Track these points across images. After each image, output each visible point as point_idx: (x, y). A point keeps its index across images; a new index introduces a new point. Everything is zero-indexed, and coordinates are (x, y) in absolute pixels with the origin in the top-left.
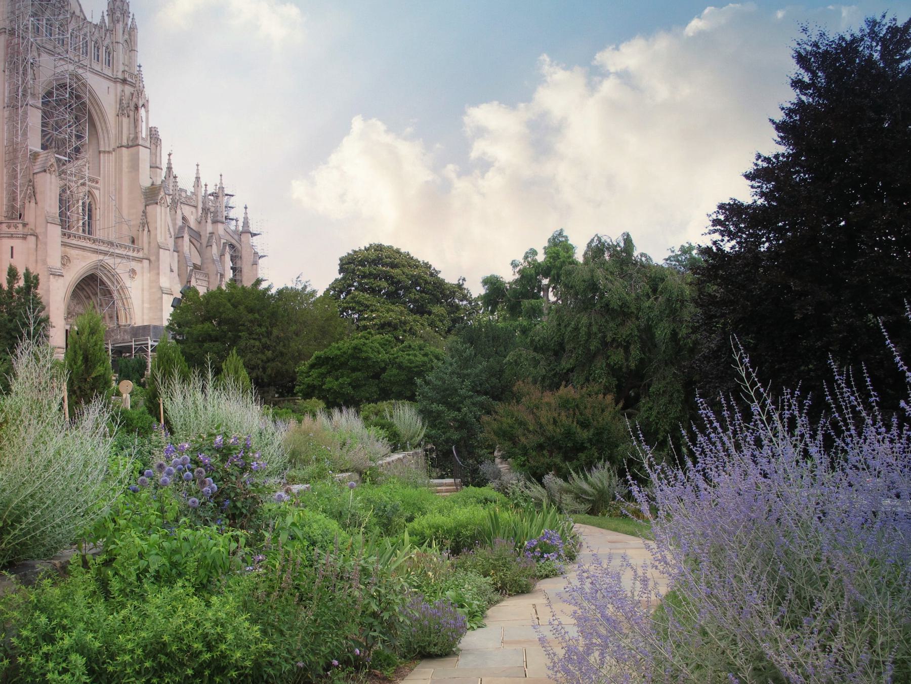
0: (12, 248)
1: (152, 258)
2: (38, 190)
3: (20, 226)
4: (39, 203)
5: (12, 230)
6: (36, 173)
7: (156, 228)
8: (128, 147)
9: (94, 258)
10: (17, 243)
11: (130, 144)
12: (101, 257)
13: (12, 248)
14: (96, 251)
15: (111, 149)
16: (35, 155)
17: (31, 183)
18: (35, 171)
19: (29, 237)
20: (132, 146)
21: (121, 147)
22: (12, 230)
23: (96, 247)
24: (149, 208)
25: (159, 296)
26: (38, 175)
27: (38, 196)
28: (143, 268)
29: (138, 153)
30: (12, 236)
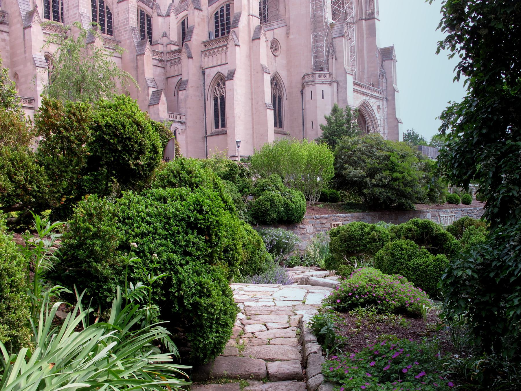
0: (323, 91)
1: (390, 98)
2: (337, 50)
3: (328, 75)
4: (339, 60)
5: (322, 79)
6: (335, 38)
7: (392, 77)
8: (366, 20)
9: (363, 98)
10: (326, 88)
11: (367, 17)
12: (367, 98)
13: (323, 91)
14: (363, 94)
15: (354, 21)
16: (332, 25)
17: (331, 44)
18: (334, 36)
19: (332, 83)
20: (369, 19)
21: (362, 19)
22: (322, 79)
23: (364, 91)
24: (386, 63)
25: (395, 124)
26: (336, 39)
27: (338, 55)
28: (383, 105)
29: (374, 24)
30: (323, 83)
